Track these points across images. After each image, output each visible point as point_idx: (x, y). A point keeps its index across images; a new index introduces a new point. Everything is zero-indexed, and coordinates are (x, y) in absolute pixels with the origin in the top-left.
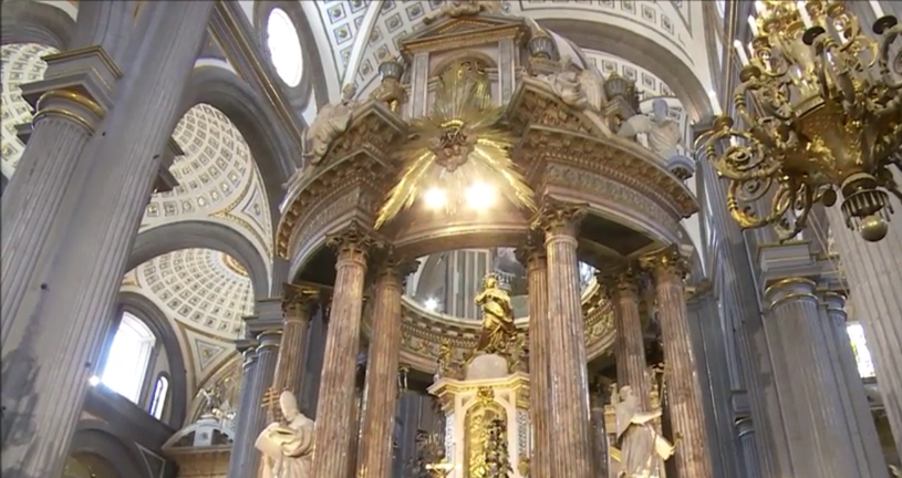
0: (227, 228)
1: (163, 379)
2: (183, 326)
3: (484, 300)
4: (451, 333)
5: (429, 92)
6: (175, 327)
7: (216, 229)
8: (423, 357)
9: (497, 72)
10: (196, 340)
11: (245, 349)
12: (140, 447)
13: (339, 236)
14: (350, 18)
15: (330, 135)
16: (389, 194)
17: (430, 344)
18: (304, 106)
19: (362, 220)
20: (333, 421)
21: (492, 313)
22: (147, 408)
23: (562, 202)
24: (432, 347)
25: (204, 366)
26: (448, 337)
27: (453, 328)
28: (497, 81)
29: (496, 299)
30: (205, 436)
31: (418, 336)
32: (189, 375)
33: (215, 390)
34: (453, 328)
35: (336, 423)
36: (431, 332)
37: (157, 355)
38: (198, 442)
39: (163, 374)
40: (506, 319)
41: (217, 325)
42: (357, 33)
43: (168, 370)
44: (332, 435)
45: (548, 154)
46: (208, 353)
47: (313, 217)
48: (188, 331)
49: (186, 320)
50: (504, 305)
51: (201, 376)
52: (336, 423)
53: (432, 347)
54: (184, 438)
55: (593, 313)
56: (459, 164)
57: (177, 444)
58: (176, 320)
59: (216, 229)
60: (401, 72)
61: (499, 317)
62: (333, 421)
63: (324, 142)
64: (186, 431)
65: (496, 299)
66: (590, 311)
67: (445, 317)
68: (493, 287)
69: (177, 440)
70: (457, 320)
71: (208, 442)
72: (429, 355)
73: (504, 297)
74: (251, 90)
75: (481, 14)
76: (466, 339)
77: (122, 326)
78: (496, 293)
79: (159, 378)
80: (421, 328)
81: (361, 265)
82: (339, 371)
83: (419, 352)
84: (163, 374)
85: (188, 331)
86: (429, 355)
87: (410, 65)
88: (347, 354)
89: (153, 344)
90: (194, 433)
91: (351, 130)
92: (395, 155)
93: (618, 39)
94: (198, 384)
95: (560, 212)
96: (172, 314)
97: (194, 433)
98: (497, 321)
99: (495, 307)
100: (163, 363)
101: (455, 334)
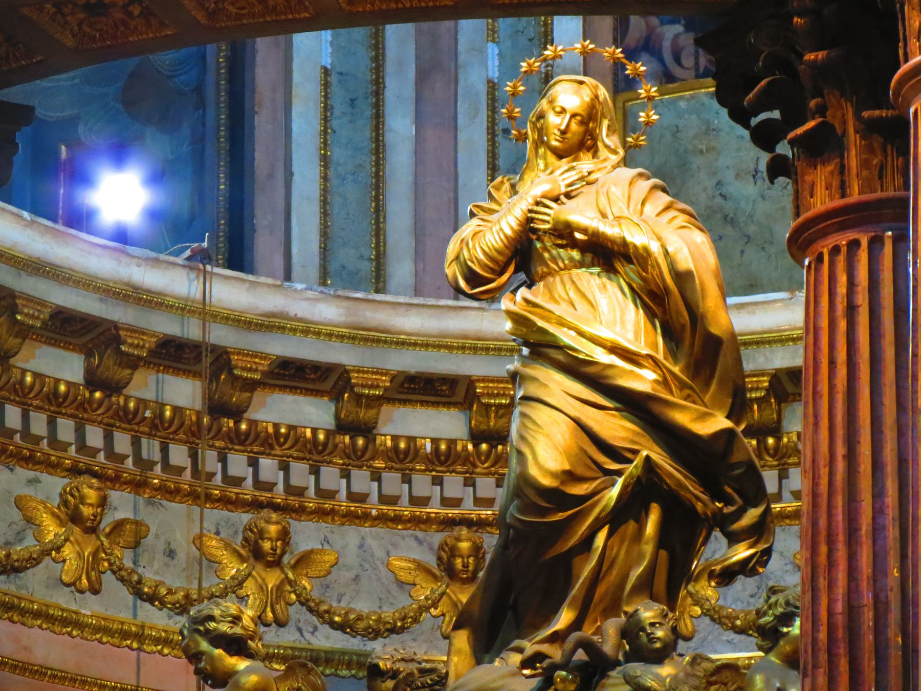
4: (280, 410)
17: (123, 505)
21: (577, 369)
24: (133, 534)
26: (263, 442)
27: (294, 375)
29: (605, 254)
34: (294, 375)
36: (126, 418)
40: (682, 418)
53: (133, 534)
61: (633, 404)
67: (230, 292)
68: (582, 143)
70: (328, 311)
72: (115, 605)
73: (683, 245)
76: (404, 457)
78: (615, 199)
83: (35, 586)
86: (115, 605)
98: (616, 427)
99: (602, 316)
101: (313, 414)
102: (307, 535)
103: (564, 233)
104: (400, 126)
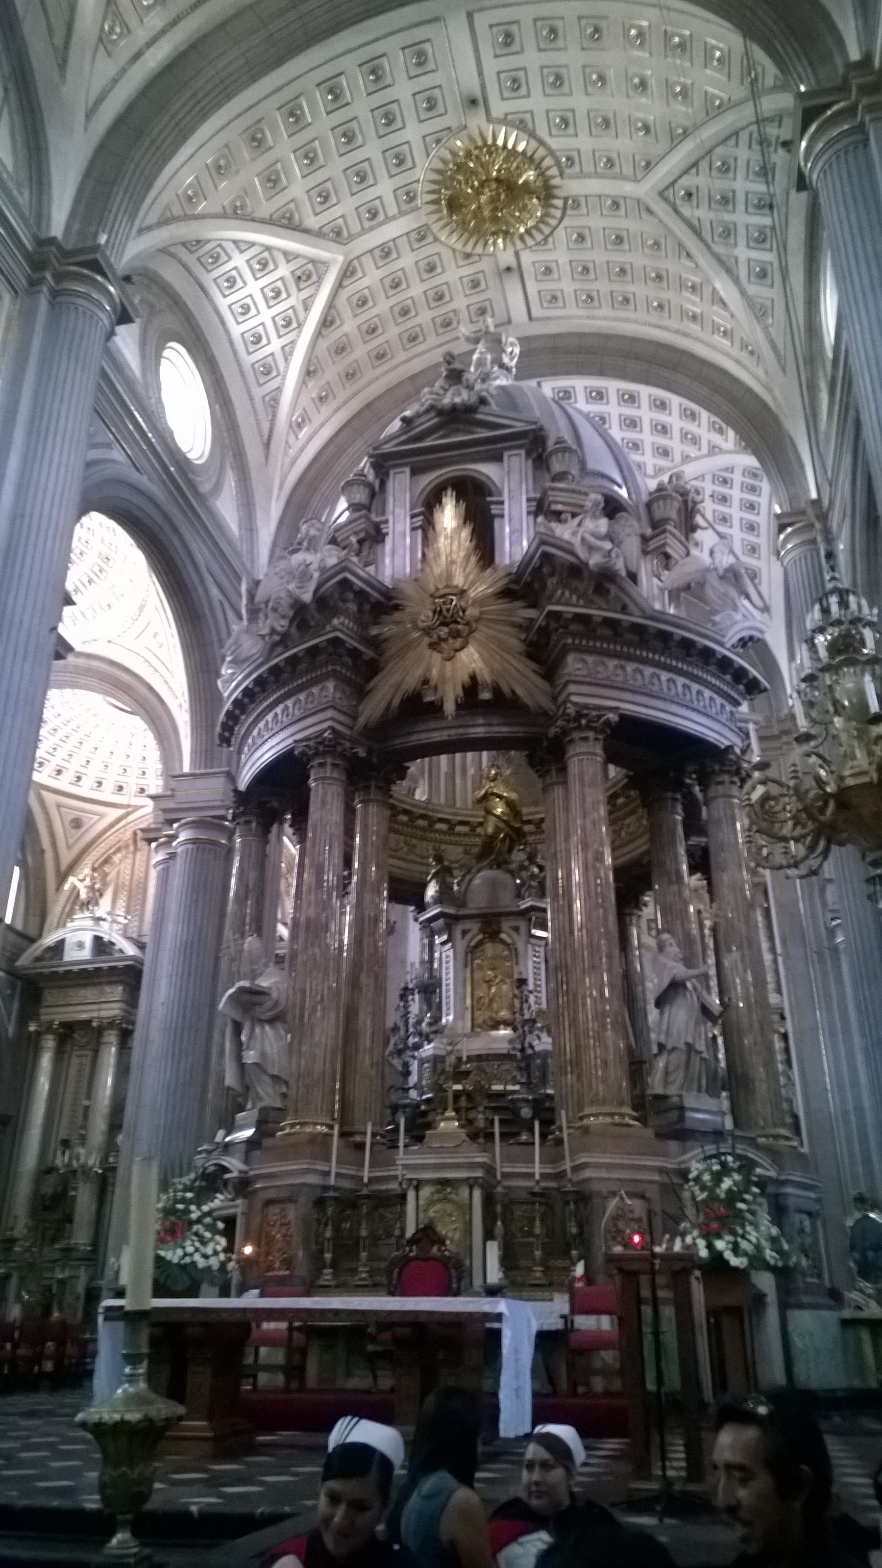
0: (112, 663)
3: (485, 797)
4: (439, 826)
5: (413, 529)
7: (95, 664)
8: (404, 860)
9: (502, 503)
10: (59, 806)
11: (155, 840)
13: (311, 743)
14: (276, 345)
15: (292, 606)
16: (372, 684)
17: (414, 841)
18: (217, 488)
19: (341, 724)
23: (586, 706)
25: (71, 841)
26: (437, 831)
27: (441, 820)
28: (502, 516)
29: (500, 797)
30: (81, 945)
31: (396, 832)
32: (49, 856)
33: (93, 878)
34: (441, 820)
38: (71, 955)
41: (88, 782)
42: (287, 367)
45: (570, 641)
46: (77, 823)
47: (271, 707)
50: (509, 804)
51: (66, 858)
53: (414, 846)
54: (49, 949)
55: (625, 805)
56: (457, 650)
57: (38, 959)
59: (95, 664)
60: (373, 495)
63: (283, 617)
64: (49, 940)
65: (500, 797)
66: (621, 801)
69: (38, 953)
71: (86, 954)
74: (149, 484)
75: (482, 409)
76: (459, 834)
80: (403, 824)
81: (335, 779)
83: (400, 854)
86: (412, 857)
87: (383, 484)
90: (62, 942)
91: (321, 601)
92: (374, 631)
93: (675, 367)
94: (63, 867)
95: (583, 722)
97: (62, 942)
98: (502, 825)
102: (443, 847)
103: (493, 794)
104: (458, 781)
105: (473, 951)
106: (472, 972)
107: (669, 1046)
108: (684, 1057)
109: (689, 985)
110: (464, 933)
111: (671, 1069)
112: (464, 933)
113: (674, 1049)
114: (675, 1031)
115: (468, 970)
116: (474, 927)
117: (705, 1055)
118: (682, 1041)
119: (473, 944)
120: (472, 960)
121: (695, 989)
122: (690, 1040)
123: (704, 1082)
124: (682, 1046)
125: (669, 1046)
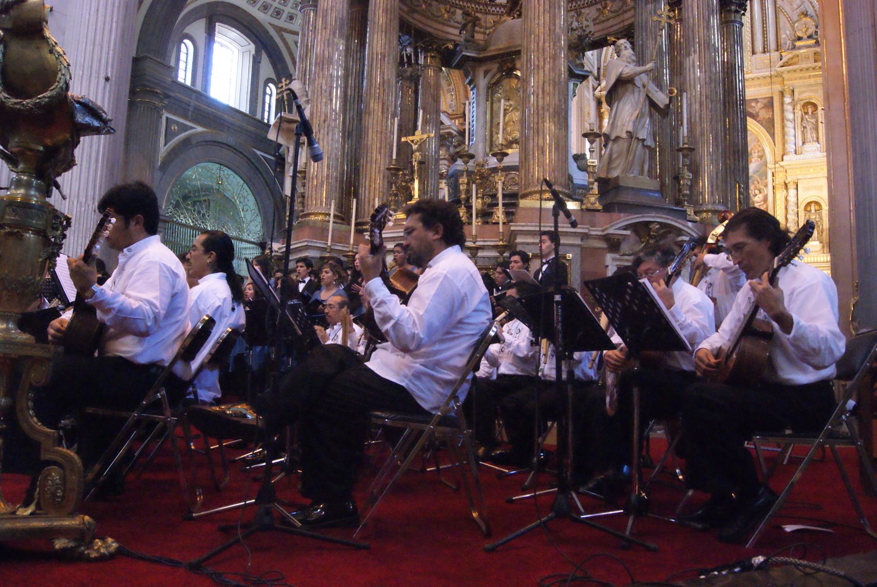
1: (270, 85)
2: (280, 30)
6: (273, 32)
12: (258, 153)
20: (323, 104)
22: (259, 117)
35: (326, 106)
37: (259, 62)
39: (269, 80)
43: (273, 76)
44: (323, 118)
48: (285, 34)
49: (282, 23)
52: (326, 106)
58: (271, 24)
62: (323, 104)
77: (218, 38)
79: (266, 85)
82: (326, 53)
84: (269, 80)
85: (285, 34)
88: (334, 33)
89: (253, 52)
96: (263, 17)
100: (266, 69)
105: (492, 88)
106: (492, 104)
107: (613, 138)
108: (626, 145)
109: (638, 83)
110: (486, 73)
111: (614, 156)
112: (486, 73)
113: (617, 138)
114: (619, 124)
115: (489, 103)
116: (495, 67)
117: (649, 142)
118: (624, 132)
119: (494, 80)
120: (493, 94)
121: (644, 86)
122: (630, 129)
123: (646, 167)
124: (624, 135)
125: (613, 138)
